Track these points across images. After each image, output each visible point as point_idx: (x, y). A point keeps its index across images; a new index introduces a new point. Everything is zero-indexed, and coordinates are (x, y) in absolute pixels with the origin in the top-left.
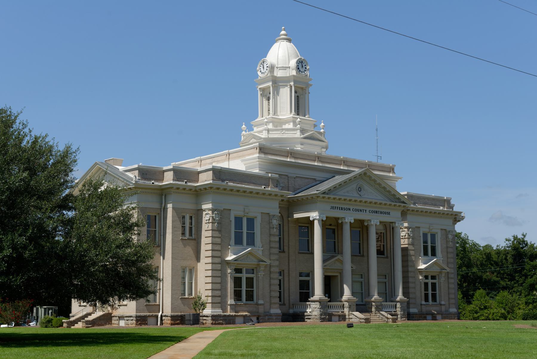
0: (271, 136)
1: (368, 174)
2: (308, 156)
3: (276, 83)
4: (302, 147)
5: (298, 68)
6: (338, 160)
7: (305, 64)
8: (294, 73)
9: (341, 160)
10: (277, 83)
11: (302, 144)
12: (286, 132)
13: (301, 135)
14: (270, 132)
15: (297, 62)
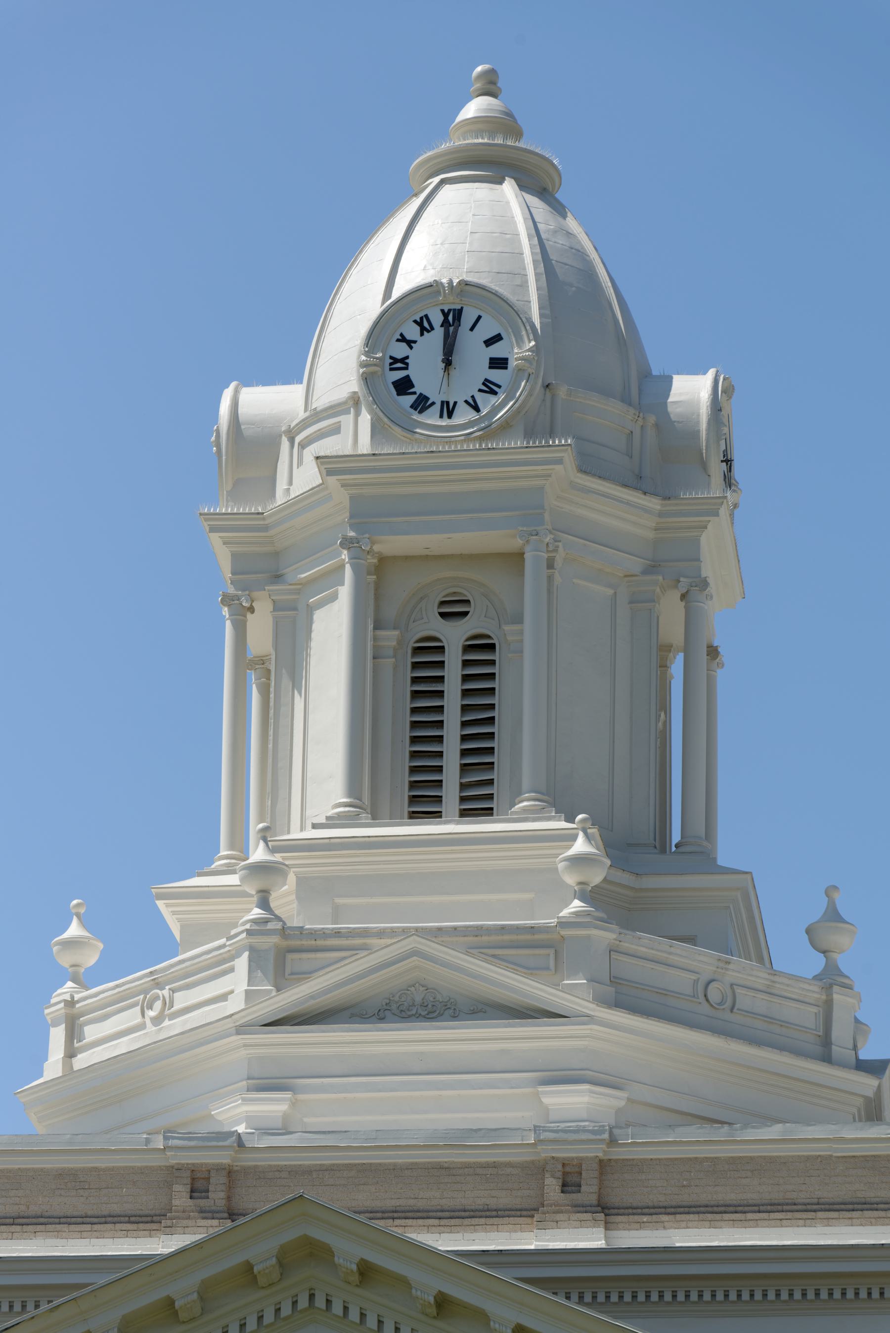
0: (81, 1061)
1: (349, 1251)
2: (70, 1179)
3: (277, 578)
4: (274, 1107)
5: (404, 386)
6: (489, 1173)
7: (487, 329)
8: (357, 436)
9: (536, 1170)
10: (266, 571)
11: (266, 1084)
12: (182, 1000)
13: (249, 995)
14: (91, 1032)
15: (375, 336)
